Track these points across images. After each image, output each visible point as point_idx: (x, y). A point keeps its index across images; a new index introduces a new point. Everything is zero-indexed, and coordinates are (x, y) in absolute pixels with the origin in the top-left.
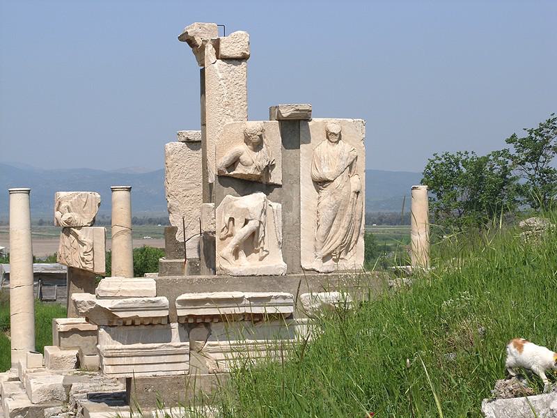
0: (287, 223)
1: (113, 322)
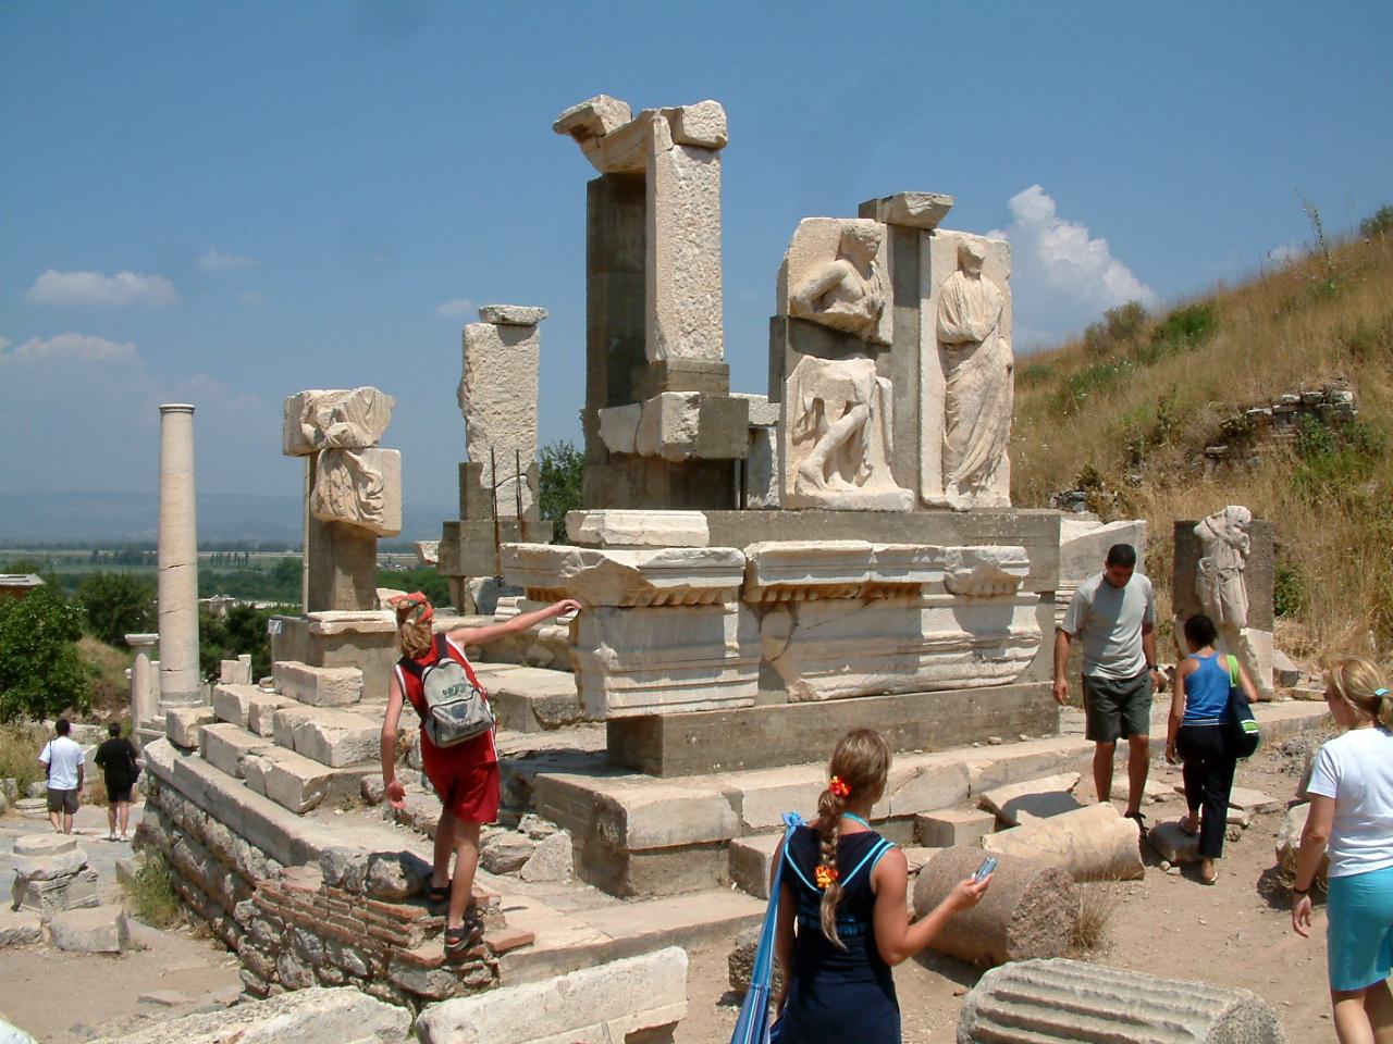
0: (899, 418)
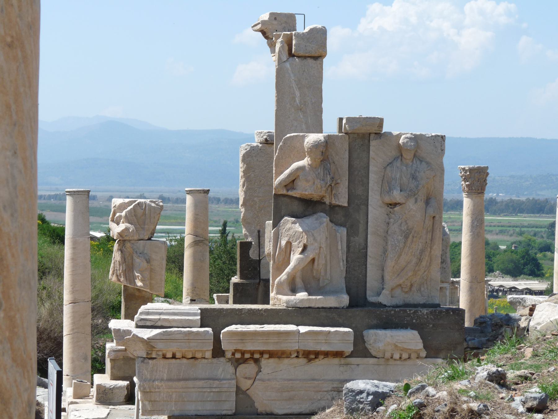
1: (151, 354)
